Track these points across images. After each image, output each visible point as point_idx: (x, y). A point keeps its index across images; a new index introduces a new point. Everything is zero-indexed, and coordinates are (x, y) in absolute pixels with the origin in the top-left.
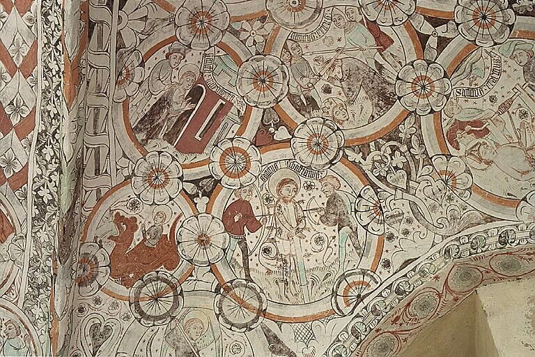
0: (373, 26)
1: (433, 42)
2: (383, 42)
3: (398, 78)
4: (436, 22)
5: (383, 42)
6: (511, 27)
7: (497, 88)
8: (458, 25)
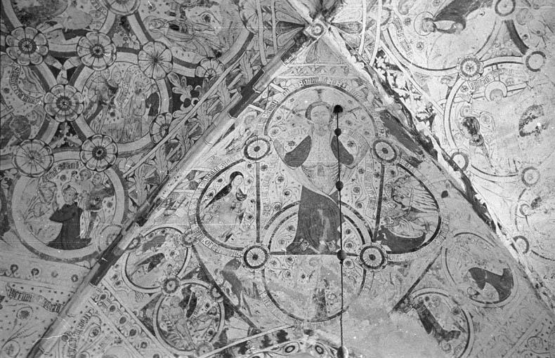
0: (82, 33)
1: (57, 65)
2: (69, 34)
3: (39, 32)
4: (70, 72)
5: (69, 34)
6: (54, 117)
7: (15, 96)
8: (64, 85)
